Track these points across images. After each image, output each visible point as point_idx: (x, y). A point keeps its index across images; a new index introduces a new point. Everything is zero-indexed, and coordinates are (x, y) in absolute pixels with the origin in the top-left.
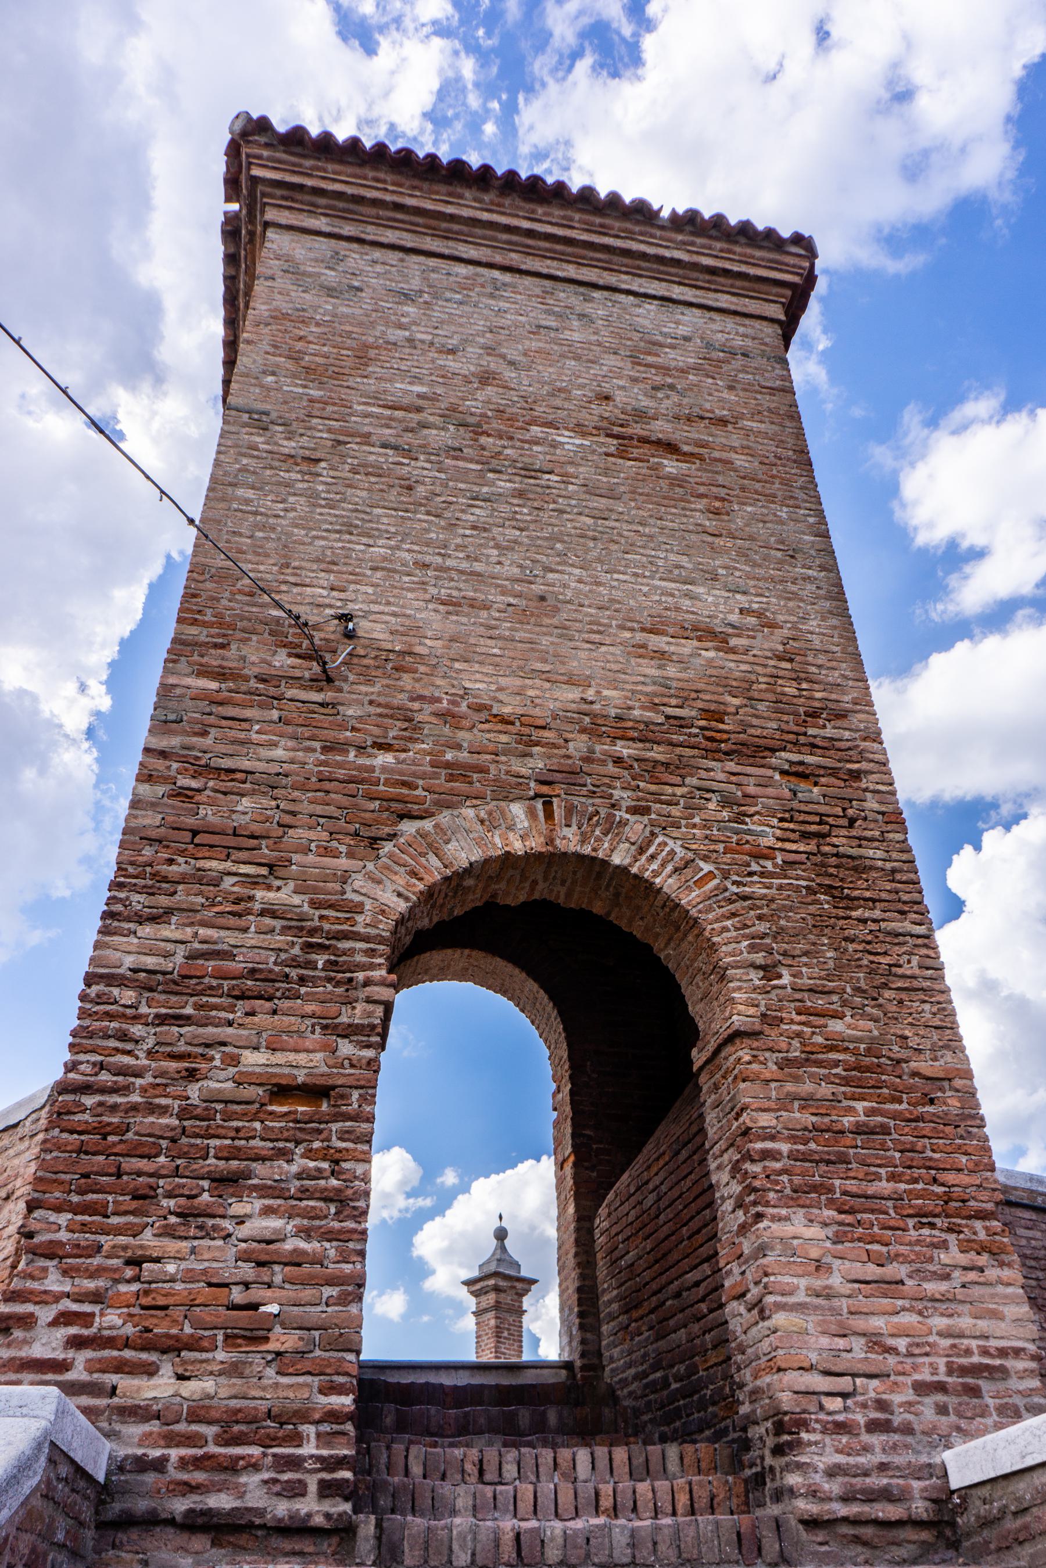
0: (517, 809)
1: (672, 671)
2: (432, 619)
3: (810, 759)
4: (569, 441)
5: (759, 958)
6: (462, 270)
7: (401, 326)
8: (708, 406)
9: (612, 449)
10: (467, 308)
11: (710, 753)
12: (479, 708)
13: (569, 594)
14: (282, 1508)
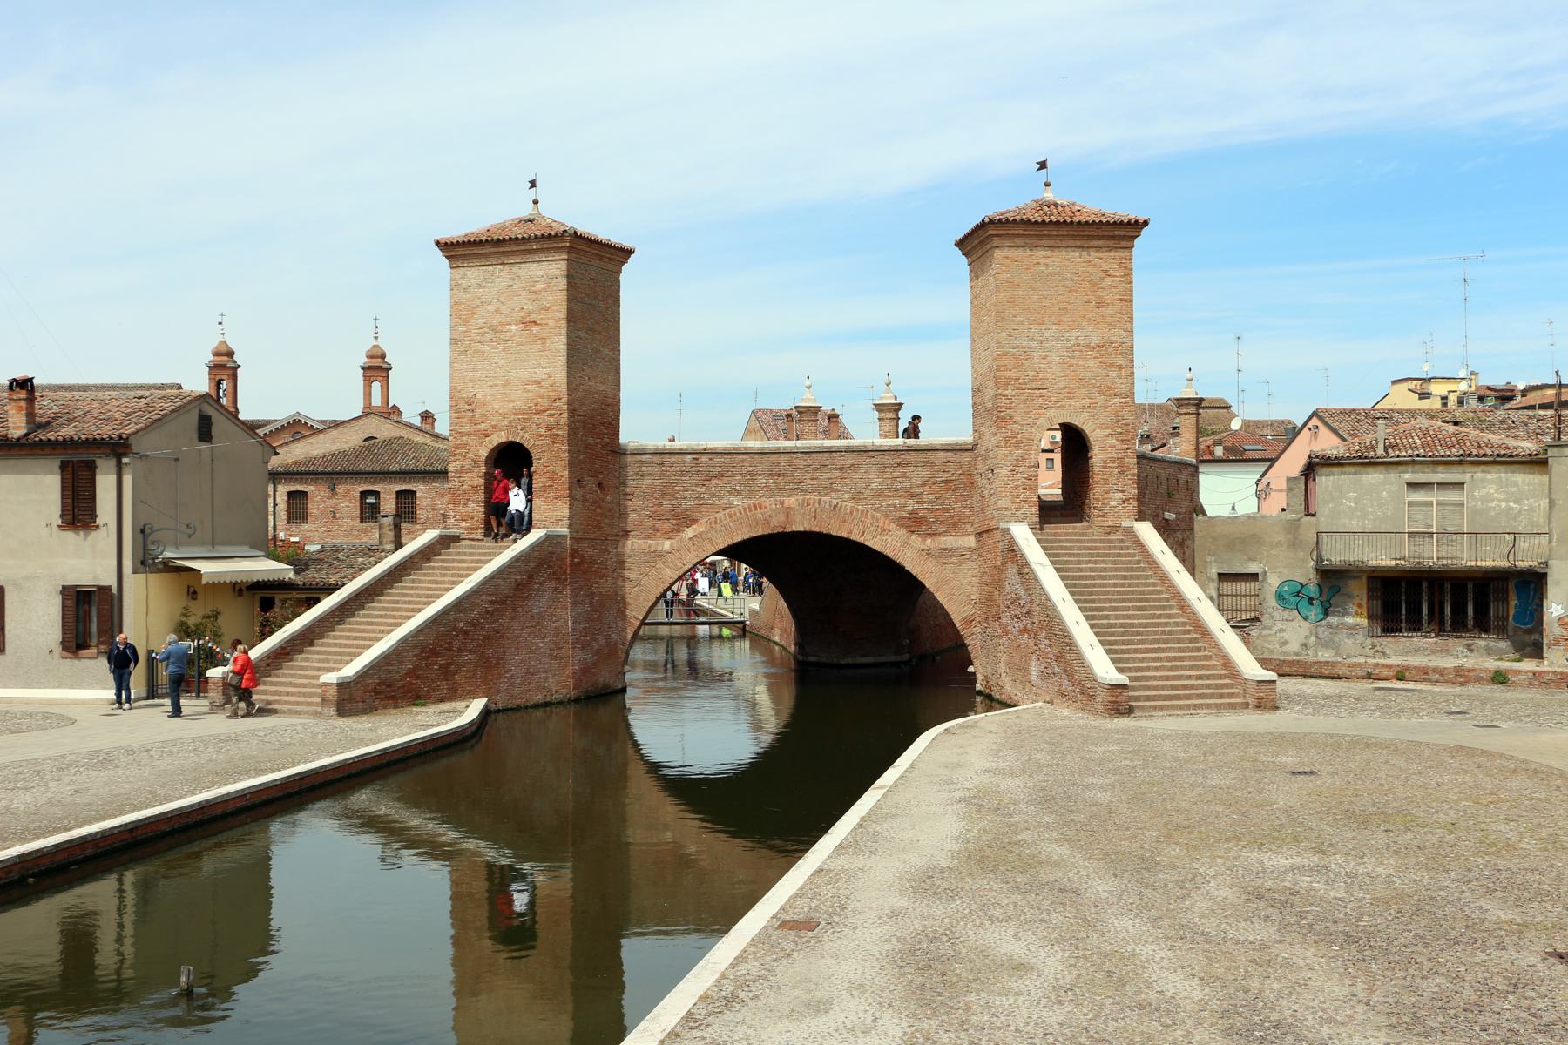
2: (488, 390)
3: (553, 412)
4: (514, 328)
6: (491, 268)
7: (480, 298)
11: (535, 414)
12: (497, 412)
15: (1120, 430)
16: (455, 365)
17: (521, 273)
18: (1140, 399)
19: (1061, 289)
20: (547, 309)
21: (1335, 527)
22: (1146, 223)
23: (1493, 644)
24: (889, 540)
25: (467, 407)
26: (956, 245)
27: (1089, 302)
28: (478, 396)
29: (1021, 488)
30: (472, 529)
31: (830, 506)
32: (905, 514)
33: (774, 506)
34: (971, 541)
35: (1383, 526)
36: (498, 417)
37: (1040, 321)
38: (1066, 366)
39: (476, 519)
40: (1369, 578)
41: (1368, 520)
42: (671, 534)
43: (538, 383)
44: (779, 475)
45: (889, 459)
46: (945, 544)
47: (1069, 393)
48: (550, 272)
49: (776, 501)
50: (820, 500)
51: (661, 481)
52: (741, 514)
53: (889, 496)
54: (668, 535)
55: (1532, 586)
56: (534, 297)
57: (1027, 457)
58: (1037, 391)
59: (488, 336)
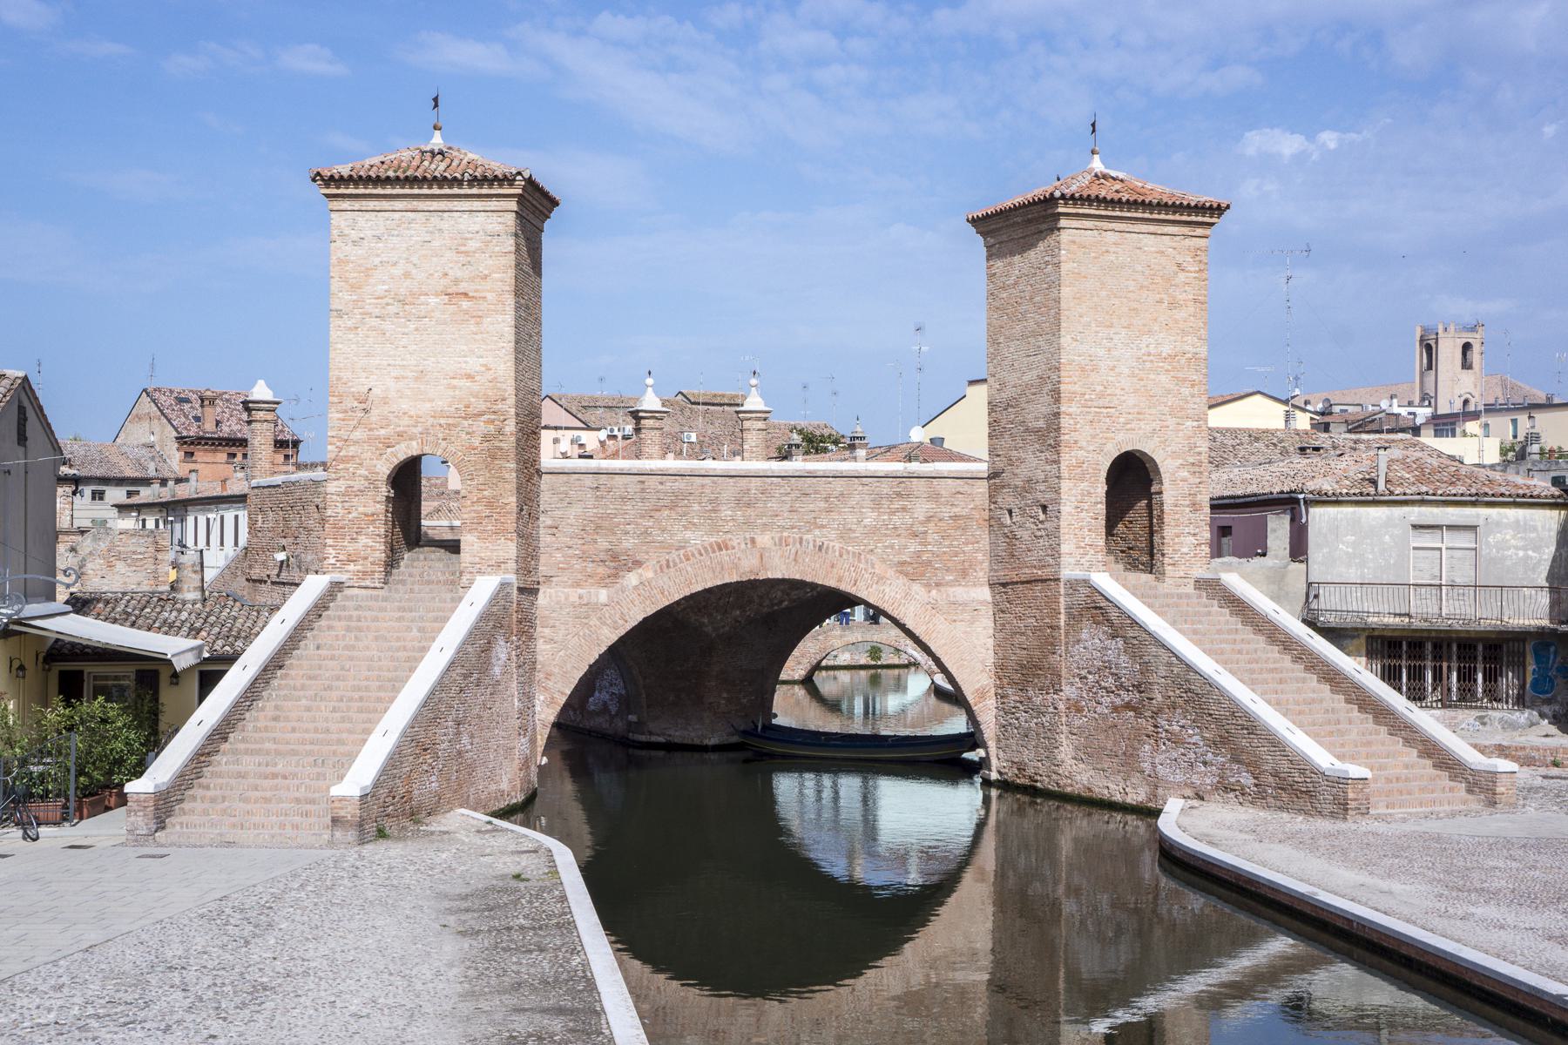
0: (414, 443)
1: (457, 393)
4: (433, 300)
5: (470, 477)
6: (397, 215)
7: (378, 256)
8: (481, 269)
9: (446, 301)
10: (399, 239)
11: (465, 418)
12: (404, 413)
13: (430, 369)
14: (372, 585)
15: (1192, 461)
16: (340, 346)
17: (445, 225)
18: (1211, 424)
19: (1132, 285)
20: (486, 277)
21: (1385, 576)
22: (1228, 207)
23: (1507, 715)
24: (887, 590)
25: (356, 404)
26: (968, 220)
27: (1160, 301)
28: (374, 390)
29: (1086, 530)
30: (365, 573)
31: (814, 546)
32: (905, 558)
33: (743, 546)
34: (985, 594)
35: (1385, 576)
36: (406, 421)
37: (1108, 323)
38: (1135, 380)
39: (371, 559)
40: (1368, 637)
41: (1368, 569)
42: (607, 581)
43: (469, 377)
44: (748, 505)
45: (886, 487)
46: (955, 596)
47: (1138, 413)
48: (490, 226)
49: (745, 539)
50: (801, 539)
51: (595, 511)
52: (701, 555)
53: (886, 535)
54: (604, 582)
55: (1552, 649)
56: (462, 259)
57: (1092, 491)
58: (1103, 410)
59: (392, 309)
